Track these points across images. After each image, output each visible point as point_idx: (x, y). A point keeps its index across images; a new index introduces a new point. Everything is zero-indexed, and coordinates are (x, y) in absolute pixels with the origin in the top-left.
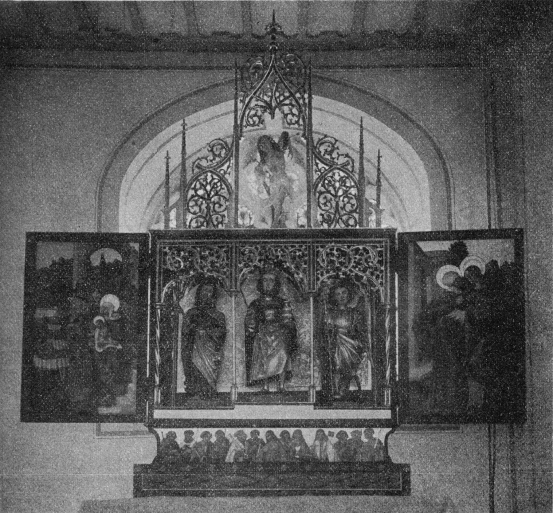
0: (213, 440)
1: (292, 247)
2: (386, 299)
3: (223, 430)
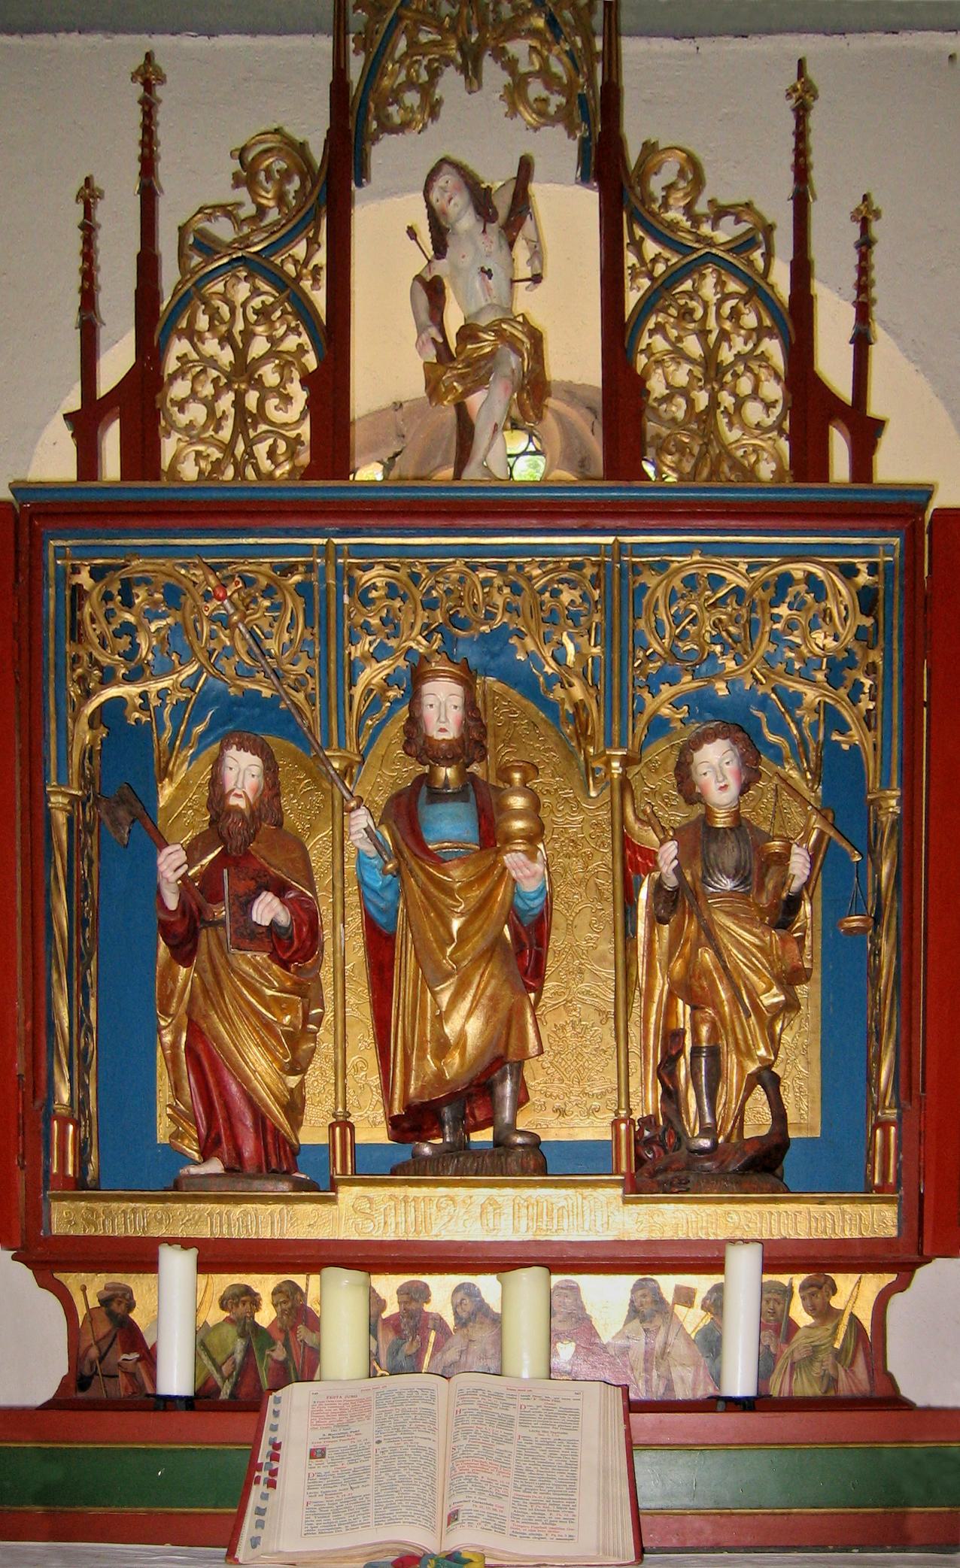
0: (266, 1316)
3: (299, 1279)
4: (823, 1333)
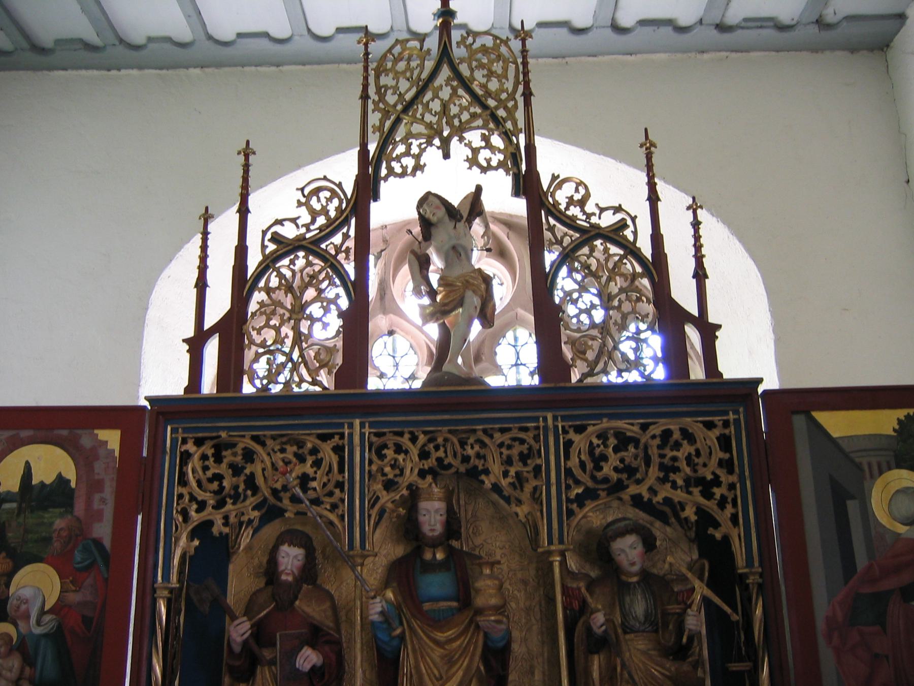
1: (503, 431)
2: (749, 562)
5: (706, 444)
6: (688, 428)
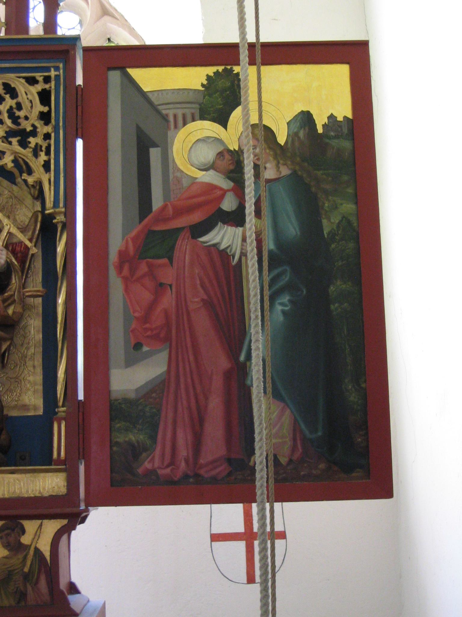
2: (56, 204)
4: (16, 561)
5: (28, 99)
6: (10, 83)
